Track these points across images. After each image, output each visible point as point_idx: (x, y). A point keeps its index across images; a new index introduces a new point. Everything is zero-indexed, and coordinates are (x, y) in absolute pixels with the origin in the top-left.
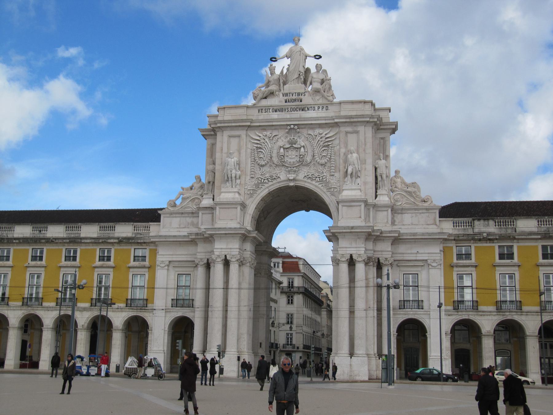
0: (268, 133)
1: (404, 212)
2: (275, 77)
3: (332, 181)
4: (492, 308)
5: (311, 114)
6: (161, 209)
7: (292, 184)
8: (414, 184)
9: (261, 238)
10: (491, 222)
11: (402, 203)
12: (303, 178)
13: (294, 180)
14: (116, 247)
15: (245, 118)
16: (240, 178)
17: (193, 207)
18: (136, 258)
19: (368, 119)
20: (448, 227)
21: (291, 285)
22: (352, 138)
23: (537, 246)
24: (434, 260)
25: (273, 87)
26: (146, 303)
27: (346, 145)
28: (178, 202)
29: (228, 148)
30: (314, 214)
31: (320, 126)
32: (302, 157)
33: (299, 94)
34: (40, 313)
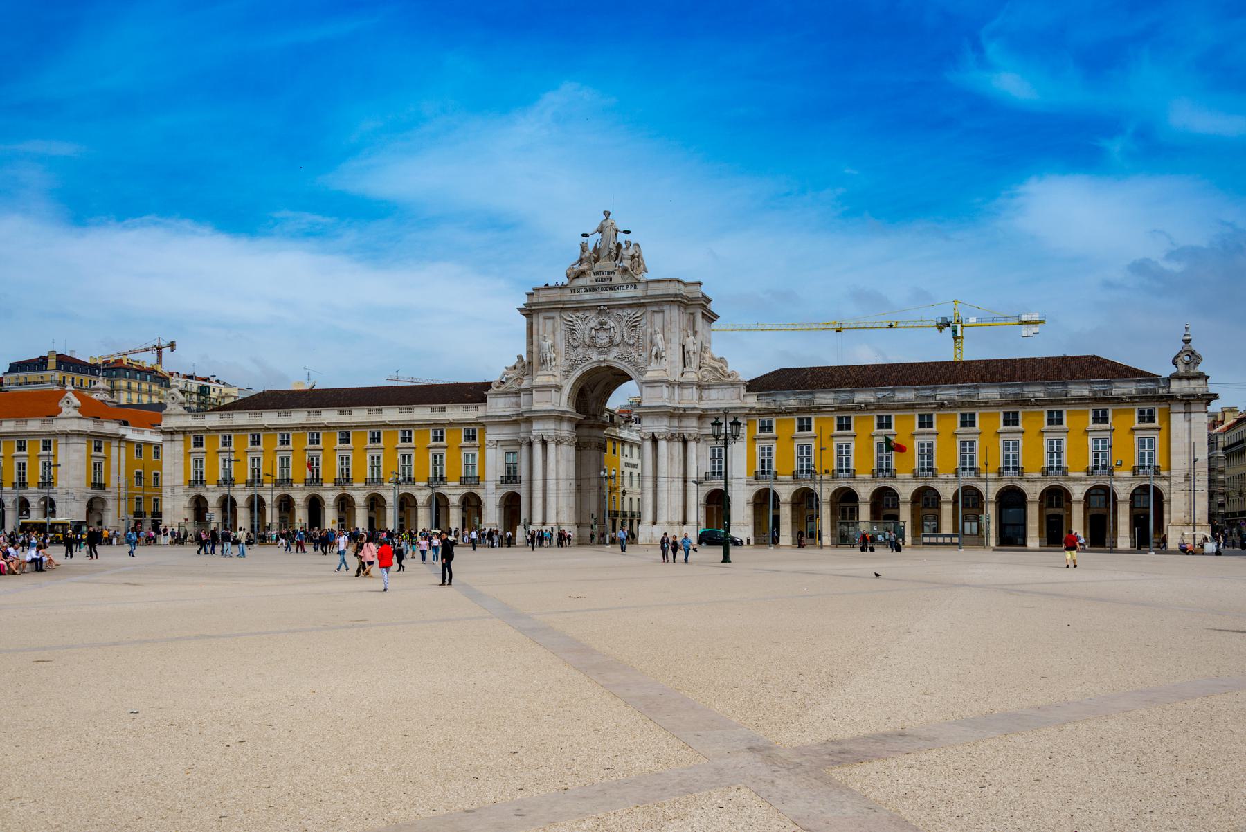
0: (580, 314)
2: (587, 254)
4: (789, 478)
5: (621, 293)
8: (722, 360)
9: (580, 417)
11: (709, 377)
12: (612, 358)
17: (514, 387)
18: (467, 438)
20: (752, 401)
22: (658, 317)
25: (584, 267)
26: (477, 481)
27: (653, 325)
29: (544, 331)
31: (629, 306)
32: (611, 338)
33: (609, 273)
34: (383, 493)
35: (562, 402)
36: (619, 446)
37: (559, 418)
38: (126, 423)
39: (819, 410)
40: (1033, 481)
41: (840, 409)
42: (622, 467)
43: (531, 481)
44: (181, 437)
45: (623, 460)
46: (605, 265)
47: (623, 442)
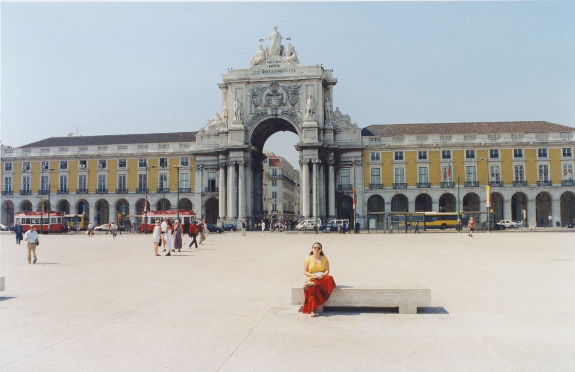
1: (342, 132)
3: (299, 115)
6: (196, 133)
7: (274, 117)
13: (276, 115)
14: (170, 158)
15: (245, 77)
16: (243, 114)
19: (319, 78)
21: (275, 174)
23: (416, 152)
24: (359, 161)
28: (206, 129)
30: (288, 133)
31: (292, 81)
33: (277, 62)
34: (127, 198)
40: (533, 188)
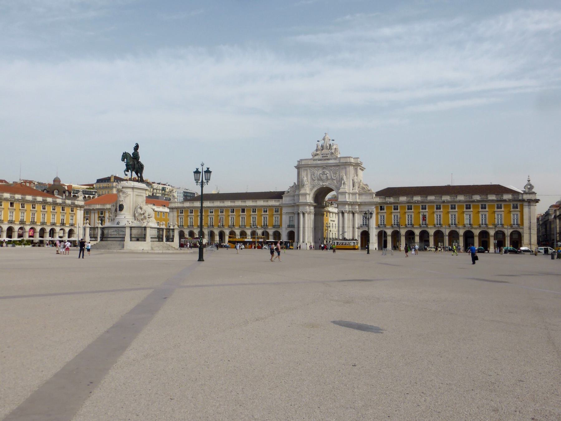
0: (316, 169)
8: (366, 185)
10: (392, 198)
18: (276, 211)
26: (279, 226)
31: (334, 166)
32: (327, 177)
35: (310, 199)
36: (328, 214)
37: (310, 205)
38: (154, 205)
39: (401, 203)
41: (408, 202)
42: (329, 221)
43: (299, 227)
44: (176, 210)
45: (330, 219)
46: (325, 151)
47: (330, 212)
